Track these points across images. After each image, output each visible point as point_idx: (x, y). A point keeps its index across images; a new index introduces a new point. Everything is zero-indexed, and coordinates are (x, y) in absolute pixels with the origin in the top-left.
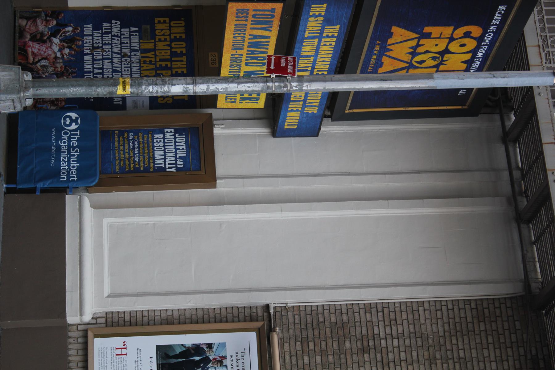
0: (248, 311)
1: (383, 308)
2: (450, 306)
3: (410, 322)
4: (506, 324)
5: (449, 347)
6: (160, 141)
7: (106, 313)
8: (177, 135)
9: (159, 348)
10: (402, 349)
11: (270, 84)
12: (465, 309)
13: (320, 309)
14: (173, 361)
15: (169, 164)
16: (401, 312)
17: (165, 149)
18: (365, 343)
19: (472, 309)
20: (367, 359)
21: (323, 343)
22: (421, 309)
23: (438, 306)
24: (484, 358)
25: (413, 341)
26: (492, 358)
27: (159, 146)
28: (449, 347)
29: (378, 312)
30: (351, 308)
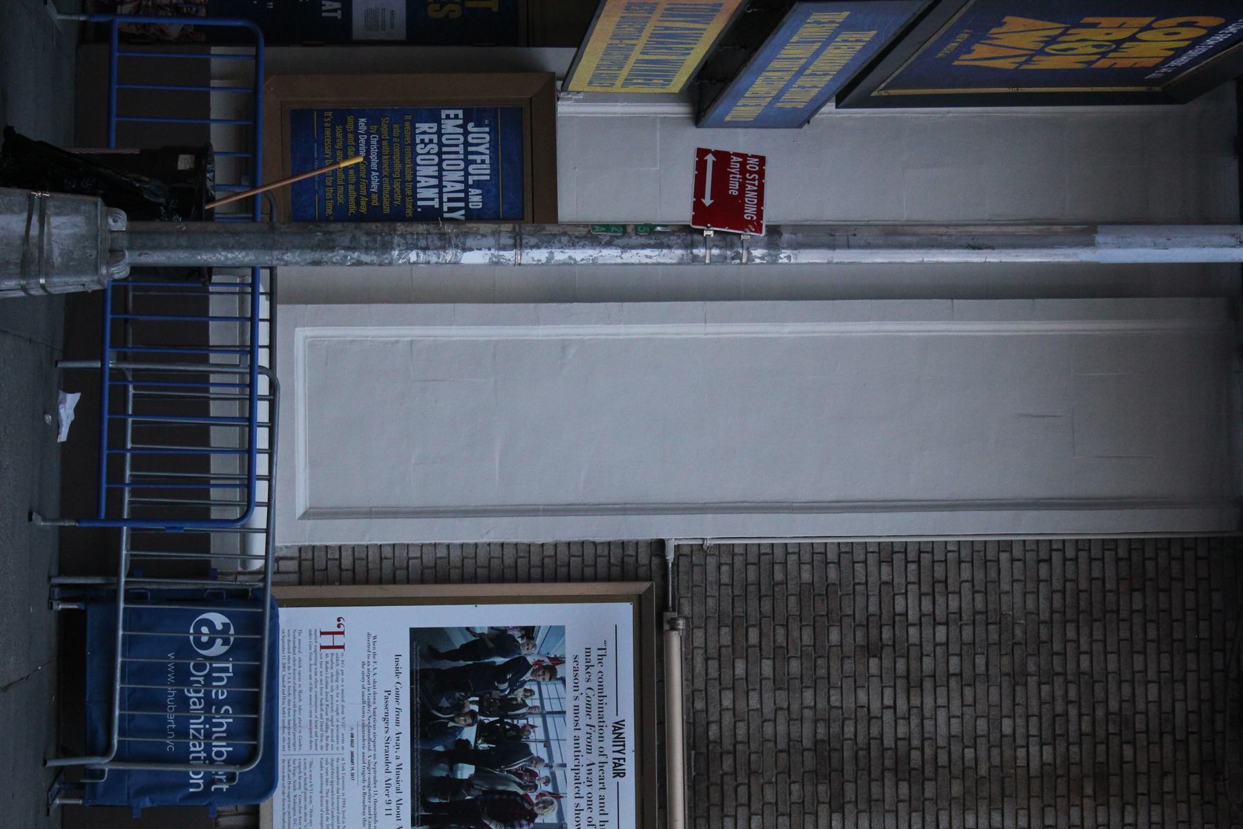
0: (616, 553)
1: (920, 552)
2: (1070, 553)
3: (977, 588)
4: (1190, 596)
5: (1057, 647)
6: (431, 141)
7: (300, 549)
8: (470, 127)
9: (418, 636)
10: (954, 648)
11: (700, 252)
12: (1103, 559)
13: (779, 554)
14: (447, 665)
15: (450, 200)
16: (960, 562)
17: (441, 161)
18: (874, 632)
19: (1118, 560)
21: (781, 631)
22: (1004, 557)
23: (1043, 552)
24: (1133, 673)
25: (980, 630)
26: (1152, 675)
27: (428, 153)
28: (1057, 647)
29: (907, 562)
30: (847, 552)
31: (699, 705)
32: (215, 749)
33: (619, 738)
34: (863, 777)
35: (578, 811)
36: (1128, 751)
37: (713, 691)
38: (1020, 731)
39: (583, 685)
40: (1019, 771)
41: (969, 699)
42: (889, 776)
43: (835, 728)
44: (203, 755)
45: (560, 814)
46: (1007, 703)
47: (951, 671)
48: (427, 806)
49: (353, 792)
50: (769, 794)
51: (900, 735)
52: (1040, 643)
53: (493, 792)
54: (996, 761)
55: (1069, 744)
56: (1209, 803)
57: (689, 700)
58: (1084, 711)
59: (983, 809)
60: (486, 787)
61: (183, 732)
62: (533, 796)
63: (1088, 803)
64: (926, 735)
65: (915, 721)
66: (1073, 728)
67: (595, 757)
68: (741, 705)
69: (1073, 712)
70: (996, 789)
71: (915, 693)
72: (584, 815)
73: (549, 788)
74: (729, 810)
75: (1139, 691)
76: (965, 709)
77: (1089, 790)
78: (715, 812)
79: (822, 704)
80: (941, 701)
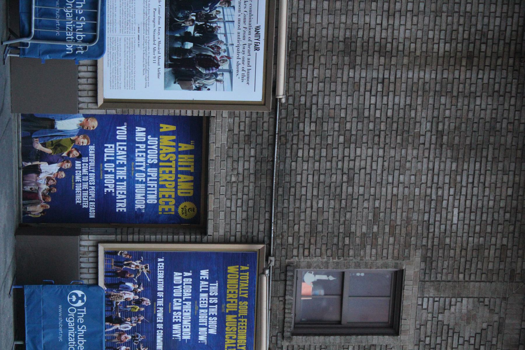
24: (490, 13)
26: (498, 14)
32: (78, 36)
33: (257, 33)
34: (365, 54)
35: (238, 64)
36: (483, 47)
37: (301, 14)
38: (437, 37)
40: (434, 54)
41: (415, 21)
42: (376, 55)
43: (354, 33)
44: (72, 38)
45: (230, 65)
46: (432, 24)
47: (408, 9)
48: (171, 60)
49: (139, 52)
50: (323, 60)
51: (383, 37)
53: (201, 55)
54: (424, 49)
55: (457, 43)
56: (516, 70)
57: (290, 18)
58: (466, 29)
59: (416, 70)
60: (198, 53)
61: (63, 28)
62: (218, 57)
63: (463, 69)
64: (394, 37)
65: (390, 31)
66: (460, 36)
67: (247, 42)
69: (461, 29)
70: (423, 61)
72: (240, 67)
73: (226, 54)
74: (305, 66)
75: (492, 20)
76: (413, 26)
77: (464, 63)
78: (298, 67)
79: (349, 22)
80: (403, 22)
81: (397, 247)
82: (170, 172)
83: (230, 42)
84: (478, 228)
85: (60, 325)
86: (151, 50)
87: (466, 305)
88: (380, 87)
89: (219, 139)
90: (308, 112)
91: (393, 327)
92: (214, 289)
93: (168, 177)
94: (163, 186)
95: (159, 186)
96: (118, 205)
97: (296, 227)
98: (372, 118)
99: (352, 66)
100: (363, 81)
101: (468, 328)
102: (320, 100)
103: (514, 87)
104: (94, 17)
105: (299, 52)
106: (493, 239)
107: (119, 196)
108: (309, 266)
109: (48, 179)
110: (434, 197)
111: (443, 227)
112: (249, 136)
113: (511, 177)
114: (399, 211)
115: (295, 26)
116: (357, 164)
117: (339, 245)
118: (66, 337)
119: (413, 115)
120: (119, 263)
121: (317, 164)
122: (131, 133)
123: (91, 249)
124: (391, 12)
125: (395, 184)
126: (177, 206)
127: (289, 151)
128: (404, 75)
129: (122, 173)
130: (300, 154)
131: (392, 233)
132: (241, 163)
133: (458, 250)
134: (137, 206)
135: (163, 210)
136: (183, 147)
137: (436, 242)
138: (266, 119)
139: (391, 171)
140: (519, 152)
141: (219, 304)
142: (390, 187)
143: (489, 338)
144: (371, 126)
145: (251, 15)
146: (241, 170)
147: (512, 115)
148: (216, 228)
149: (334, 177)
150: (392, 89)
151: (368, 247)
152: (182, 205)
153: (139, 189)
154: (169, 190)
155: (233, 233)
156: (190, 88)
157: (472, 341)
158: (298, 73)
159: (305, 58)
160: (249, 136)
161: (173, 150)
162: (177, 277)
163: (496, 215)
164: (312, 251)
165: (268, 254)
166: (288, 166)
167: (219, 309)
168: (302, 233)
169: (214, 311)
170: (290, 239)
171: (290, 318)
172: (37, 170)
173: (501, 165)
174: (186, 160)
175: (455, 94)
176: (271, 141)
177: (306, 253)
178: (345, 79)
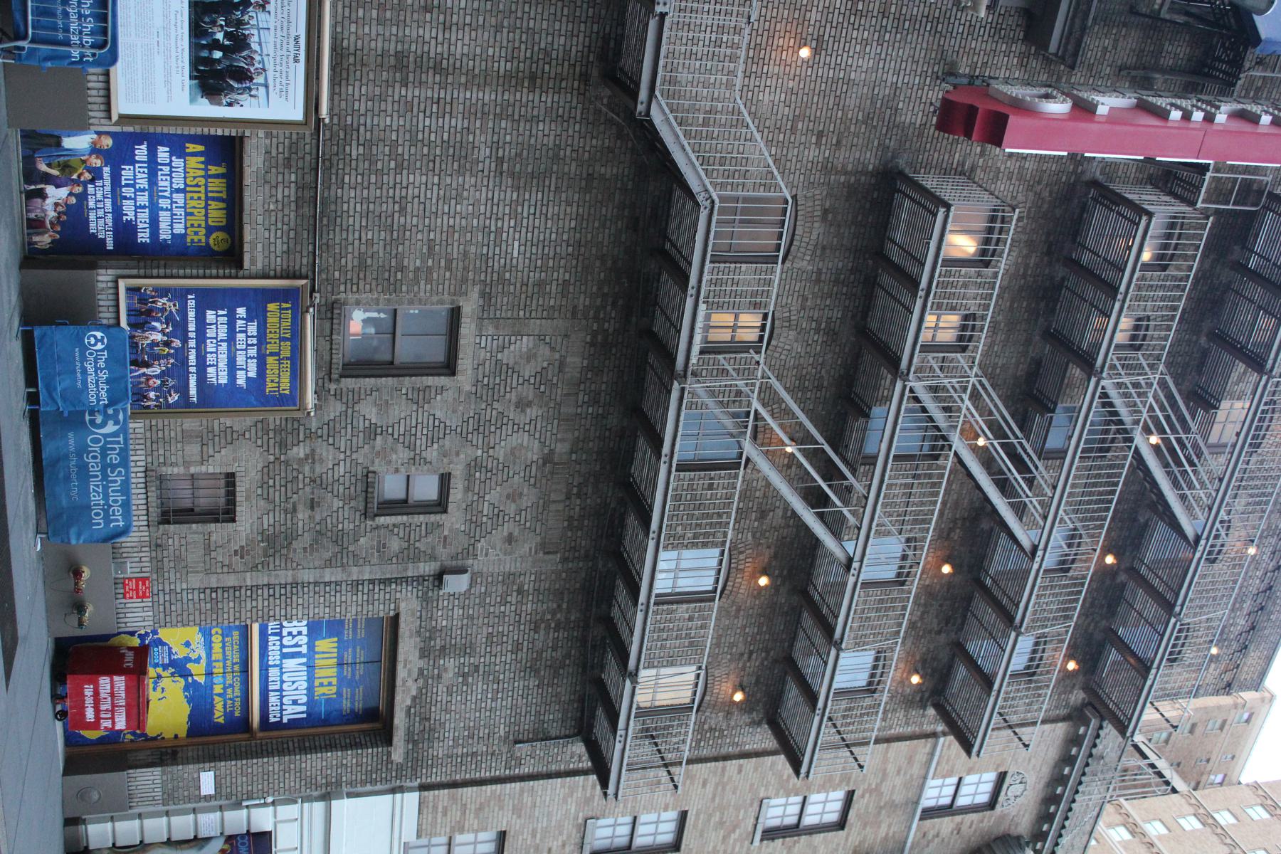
5: (519, 15)
10: (468, 12)
20: (428, 18)
26: (563, 32)
28: (519, 15)
31: (339, 30)
33: (297, 43)
34: (418, 70)
35: (275, 78)
37: (346, 23)
39: (279, 16)
42: (431, 72)
43: (406, 46)
45: (266, 79)
46: (492, 40)
48: (198, 71)
49: (159, 61)
50: (371, 76)
52: (511, 12)
53: (231, 66)
59: (475, 90)
61: (66, 30)
62: (252, 69)
63: (525, 90)
65: (446, 45)
67: (285, 53)
68: (360, 32)
69: (523, 47)
70: (482, 81)
71: (447, 32)
72: (278, 81)
74: (351, 82)
75: (556, 39)
77: (526, 84)
78: (344, 82)
79: (400, 34)
80: (460, 37)
81: (453, 282)
82: (199, 198)
83: (265, 52)
84: (539, 262)
85: (78, 370)
86: (174, 59)
87: (526, 343)
88: (435, 106)
89: (254, 161)
90: (355, 133)
91: (449, 367)
92: (253, 329)
93: (197, 204)
94: (192, 214)
95: (187, 214)
96: (140, 235)
97: (343, 260)
98: (426, 142)
99: (404, 84)
100: (416, 100)
101: (528, 367)
102: (369, 121)
103: (579, 112)
104: (104, 18)
105: (345, 66)
106: (555, 274)
107: (141, 226)
108: (358, 303)
109: (56, 205)
110: (493, 228)
111: (502, 261)
112: (289, 159)
113: (575, 209)
114: (456, 244)
115: (340, 36)
116: (410, 192)
117: (389, 280)
118: (85, 382)
119: (471, 139)
120: (143, 300)
121: (365, 192)
122: (152, 154)
123: (110, 285)
124: (447, 24)
125: (452, 214)
126: (208, 236)
127: (334, 177)
128: (462, 95)
129: (143, 199)
130: (347, 179)
131: (448, 268)
132: (280, 190)
133: (518, 285)
134: (162, 237)
135: (192, 241)
136: (214, 170)
137: (495, 278)
138: (308, 140)
139: (447, 200)
140: (583, 183)
141: (259, 345)
142: (445, 218)
143: (550, 377)
144: (425, 150)
145: (289, 22)
146: (280, 197)
147: (576, 142)
148: (253, 262)
149: (384, 206)
150: (448, 110)
151: (423, 283)
152: (214, 236)
153: (164, 218)
154: (199, 219)
155: (272, 266)
156: (220, 104)
157: (532, 381)
158: (343, 89)
159: (351, 74)
160: (289, 159)
161: (202, 173)
162: (210, 316)
163: (558, 249)
164: (361, 286)
165: (313, 290)
166: (333, 193)
167: (259, 350)
168: (349, 267)
169: (253, 352)
170: (337, 274)
171: (338, 359)
172: (42, 195)
173: (564, 195)
174: (217, 185)
175: (516, 117)
176: (314, 165)
177: (355, 289)
178: (396, 98)
